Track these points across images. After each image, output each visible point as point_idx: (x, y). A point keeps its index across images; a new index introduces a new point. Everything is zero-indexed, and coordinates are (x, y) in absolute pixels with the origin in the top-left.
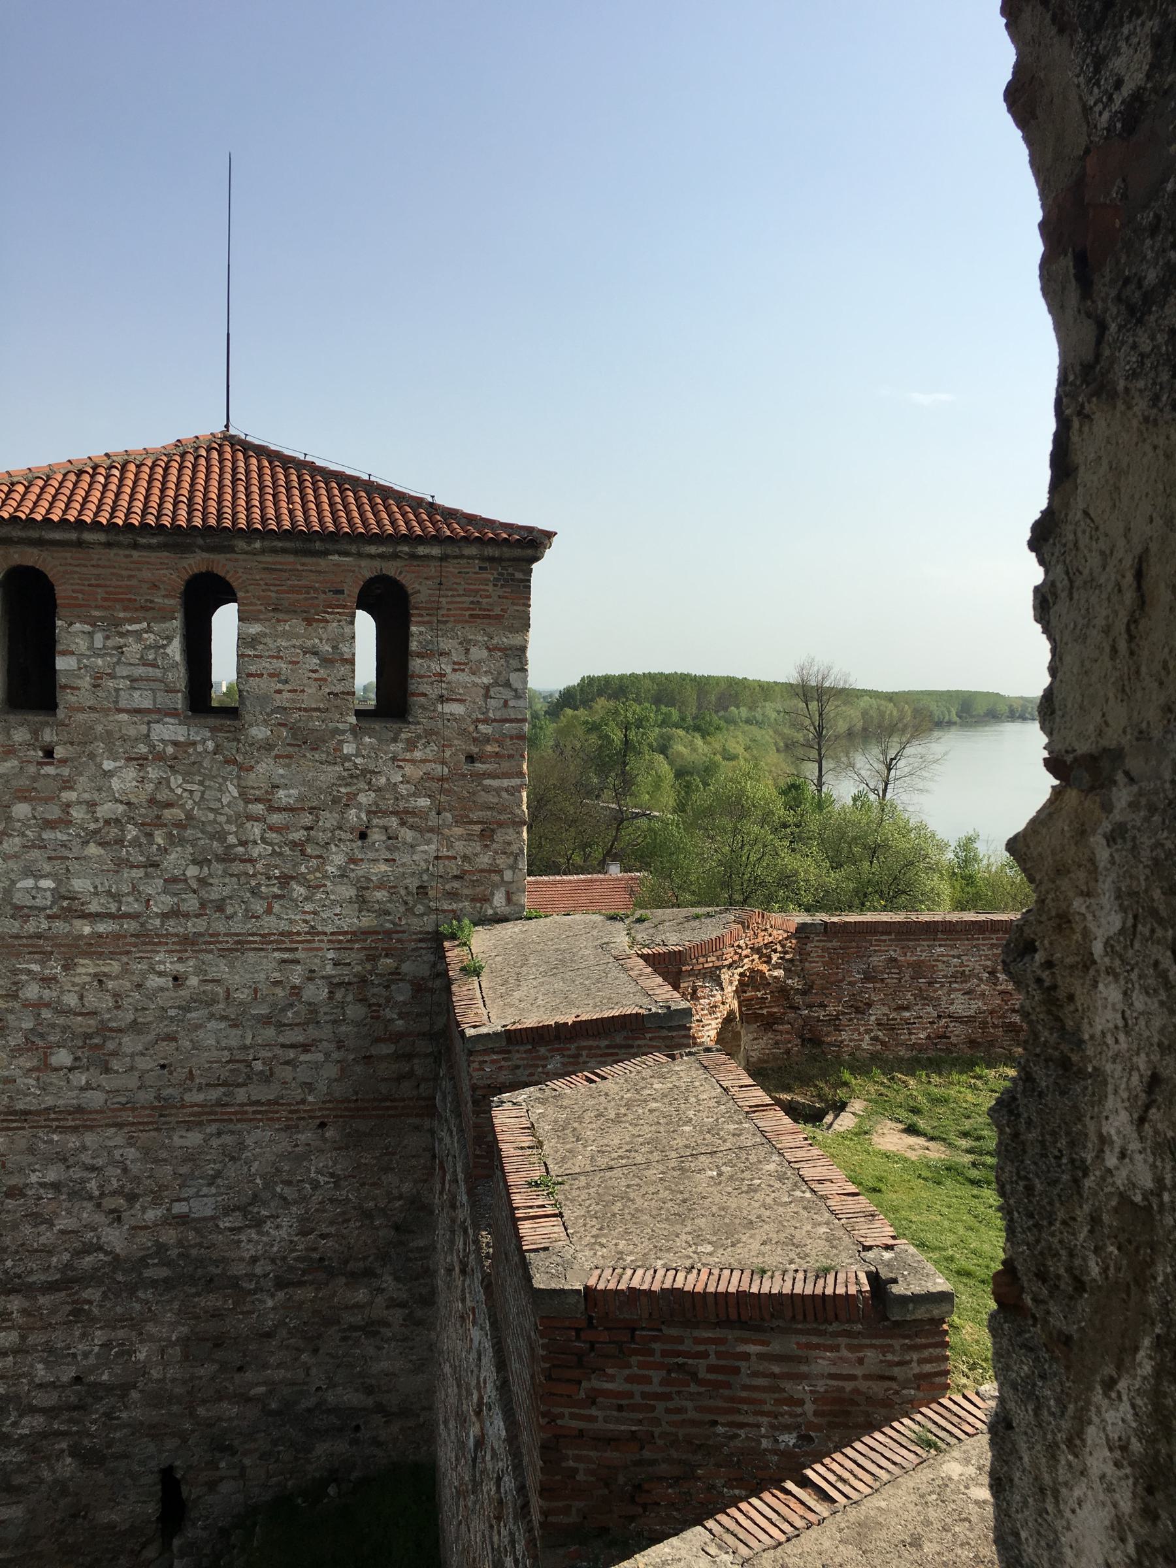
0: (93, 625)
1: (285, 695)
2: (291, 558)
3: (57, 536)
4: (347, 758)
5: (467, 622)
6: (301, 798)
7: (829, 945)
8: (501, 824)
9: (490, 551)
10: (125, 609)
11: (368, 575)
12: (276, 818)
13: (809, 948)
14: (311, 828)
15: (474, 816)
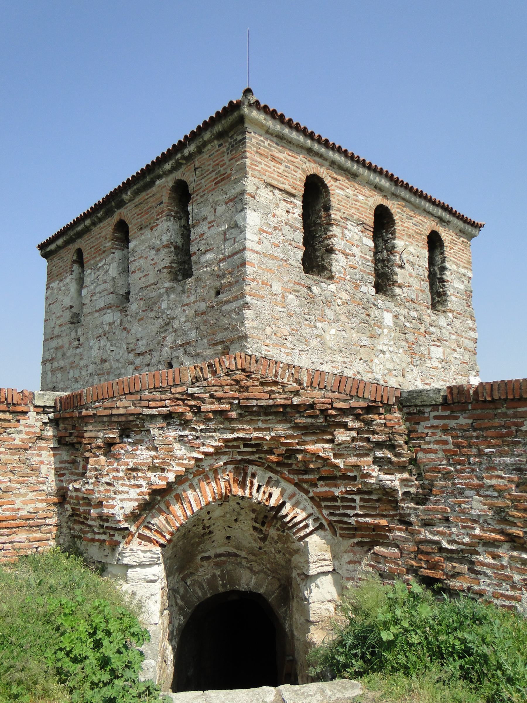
0: (91, 269)
1: (143, 279)
2: (144, 194)
3: (79, 228)
4: (163, 312)
5: (214, 189)
6: (147, 345)
7: (452, 423)
8: (232, 341)
9: (218, 128)
10: (100, 255)
11: (171, 184)
12: (138, 361)
13: (421, 429)
14: (148, 365)
15: (218, 338)
